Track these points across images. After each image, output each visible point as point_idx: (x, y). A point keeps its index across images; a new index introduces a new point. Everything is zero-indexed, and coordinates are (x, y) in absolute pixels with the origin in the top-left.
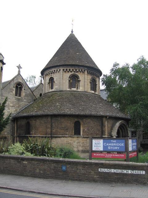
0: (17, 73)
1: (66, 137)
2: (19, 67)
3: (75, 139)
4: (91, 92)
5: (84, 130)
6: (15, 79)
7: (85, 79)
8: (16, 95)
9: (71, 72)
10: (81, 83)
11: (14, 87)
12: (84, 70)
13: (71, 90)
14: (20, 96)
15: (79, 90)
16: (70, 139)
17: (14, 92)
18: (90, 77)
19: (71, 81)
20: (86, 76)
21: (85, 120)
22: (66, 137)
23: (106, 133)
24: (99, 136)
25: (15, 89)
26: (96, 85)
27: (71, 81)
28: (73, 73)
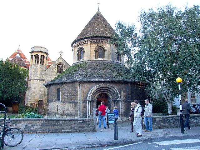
0: (60, 56)
1: (53, 102)
2: (61, 52)
3: (57, 104)
4: (96, 59)
5: (62, 95)
6: (57, 61)
7: (89, 49)
8: (58, 72)
9: (79, 45)
10: (85, 54)
11: (56, 67)
12: (88, 41)
13: (79, 61)
14: (61, 71)
15: (84, 60)
16: (54, 103)
17: (56, 71)
18: (94, 46)
19: (80, 54)
20: (89, 46)
21: (63, 87)
22: (53, 102)
23: (78, 98)
24: (73, 101)
25: (56, 68)
26: (104, 52)
27: (80, 54)
28: (80, 46)
